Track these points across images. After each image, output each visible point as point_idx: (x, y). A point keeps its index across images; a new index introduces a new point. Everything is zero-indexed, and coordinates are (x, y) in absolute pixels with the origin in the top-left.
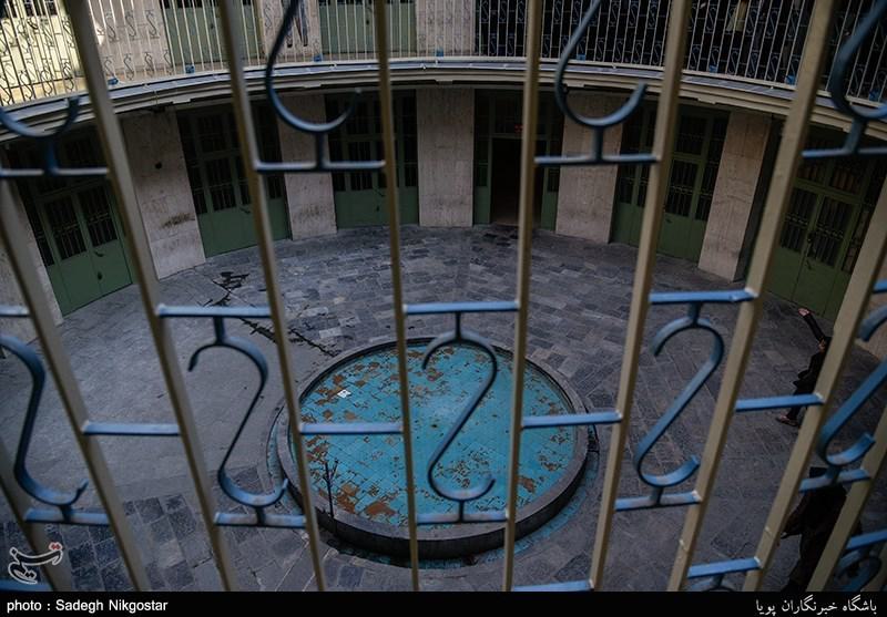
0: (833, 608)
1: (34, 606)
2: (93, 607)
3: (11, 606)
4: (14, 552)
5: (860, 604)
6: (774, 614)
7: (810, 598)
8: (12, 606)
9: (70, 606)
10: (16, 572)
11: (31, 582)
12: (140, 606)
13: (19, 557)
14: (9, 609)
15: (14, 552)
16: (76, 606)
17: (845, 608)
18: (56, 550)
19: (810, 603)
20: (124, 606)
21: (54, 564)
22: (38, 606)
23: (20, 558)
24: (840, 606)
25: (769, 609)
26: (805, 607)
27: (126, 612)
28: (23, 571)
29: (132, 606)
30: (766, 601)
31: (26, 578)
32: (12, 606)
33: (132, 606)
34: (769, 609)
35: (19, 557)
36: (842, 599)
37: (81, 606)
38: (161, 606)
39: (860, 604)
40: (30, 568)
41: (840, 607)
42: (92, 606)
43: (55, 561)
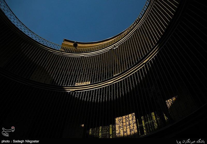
0: (194, 142)
1: (8, 141)
2: (22, 142)
3: (3, 142)
4: (3, 129)
5: (201, 141)
6: (181, 143)
7: (189, 140)
8: (3, 141)
9: (16, 142)
10: (4, 133)
11: (8, 136)
12: (33, 141)
13: (4, 130)
14: (2, 142)
15: (3, 129)
16: (18, 142)
17: (197, 142)
18: (13, 128)
19: (189, 141)
20: (29, 141)
21: (13, 132)
22: (9, 141)
23: (5, 130)
24: (196, 141)
25: (180, 142)
26: (188, 142)
27: (29, 143)
28: (5, 133)
29: (31, 142)
31: (6, 135)
32: (3, 141)
33: (31, 142)
34: (180, 142)
35: (4, 130)
37: (19, 141)
38: (38, 142)
39: (201, 141)
40: (7, 133)
41: (196, 142)
42: (21, 142)
43: (13, 131)
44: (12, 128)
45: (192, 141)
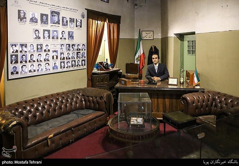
1: (10, 162)
4: (3, 148)
5: (233, 161)
8: (4, 162)
10: (4, 154)
11: (8, 156)
13: (5, 150)
14: (3, 163)
15: (3, 148)
18: (15, 148)
19: (218, 161)
21: (14, 152)
23: (6, 150)
25: (207, 163)
27: (36, 164)
28: (6, 154)
30: (206, 160)
32: (4, 162)
34: (207, 163)
35: (5, 150)
36: (228, 160)
39: (233, 161)
40: (8, 153)
43: (15, 151)
44: (14, 147)
45: (222, 160)
